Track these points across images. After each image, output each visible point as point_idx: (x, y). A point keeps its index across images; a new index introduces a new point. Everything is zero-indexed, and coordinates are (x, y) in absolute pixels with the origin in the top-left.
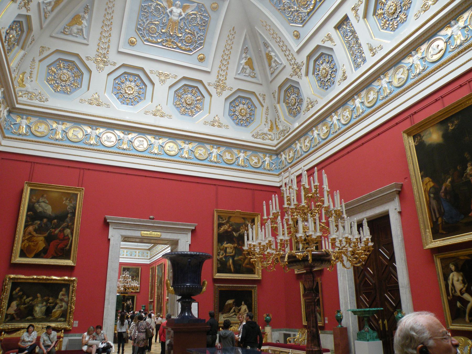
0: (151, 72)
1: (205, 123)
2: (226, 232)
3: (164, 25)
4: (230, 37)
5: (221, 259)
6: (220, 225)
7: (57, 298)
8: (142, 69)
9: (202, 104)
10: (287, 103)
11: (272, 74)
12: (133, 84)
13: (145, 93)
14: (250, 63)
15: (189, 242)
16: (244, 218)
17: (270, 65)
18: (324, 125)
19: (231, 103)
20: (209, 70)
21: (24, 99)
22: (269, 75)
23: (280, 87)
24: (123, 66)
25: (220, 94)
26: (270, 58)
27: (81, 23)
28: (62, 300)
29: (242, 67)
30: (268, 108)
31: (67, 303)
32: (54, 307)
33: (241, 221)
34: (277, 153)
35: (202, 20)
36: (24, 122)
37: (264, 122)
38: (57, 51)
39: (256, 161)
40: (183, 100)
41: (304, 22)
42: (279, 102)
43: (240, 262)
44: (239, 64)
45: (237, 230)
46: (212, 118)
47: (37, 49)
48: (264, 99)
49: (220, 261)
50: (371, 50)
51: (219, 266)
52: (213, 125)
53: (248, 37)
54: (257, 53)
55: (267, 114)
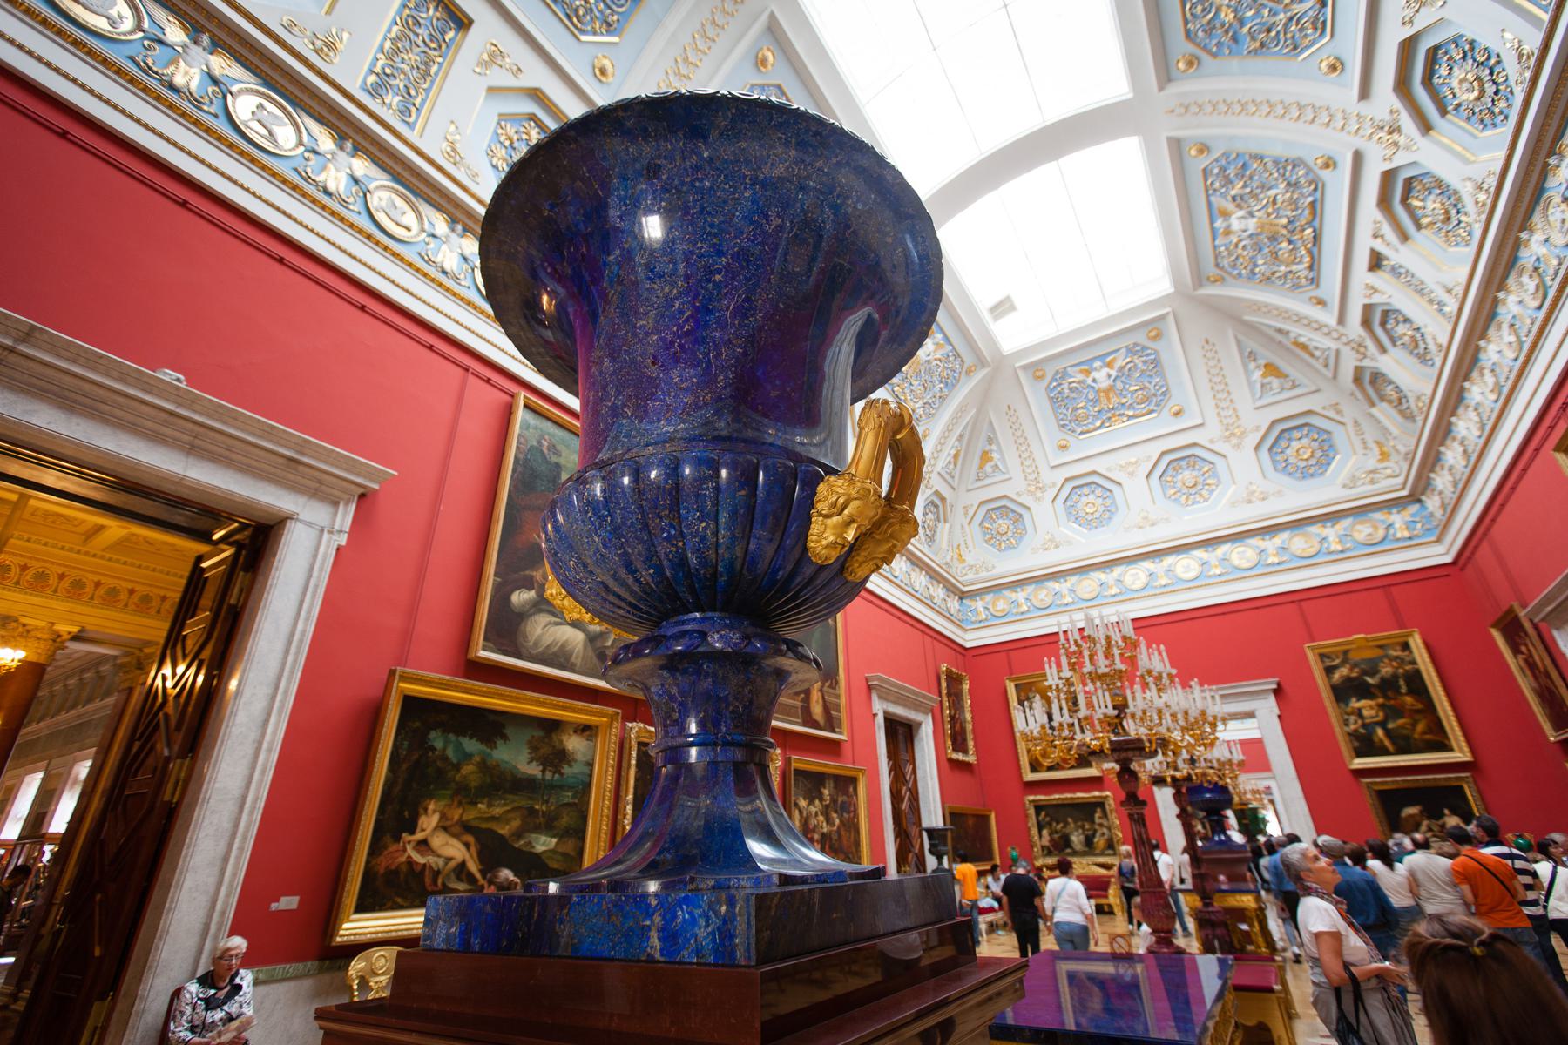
0: (1109, 469)
1: (1233, 504)
2: (1348, 679)
3: (1095, 401)
4: (1209, 355)
5: (1356, 730)
6: (1329, 671)
7: (1093, 822)
8: (1094, 472)
9: (1215, 475)
10: (1390, 402)
11: (1326, 366)
12: (1092, 497)
13: (1114, 503)
14: (1271, 369)
15: (1277, 711)
16: (1380, 647)
17: (1312, 355)
18: (1454, 439)
19: (1270, 450)
20: (1199, 421)
21: (970, 576)
22: (1324, 370)
23: (1357, 380)
24: (1067, 480)
25: (1238, 446)
26: (1304, 347)
27: (991, 459)
28: (1101, 825)
29: (1258, 386)
30: (1356, 423)
31: (1109, 829)
32: (1094, 835)
33: (1379, 652)
34: (1415, 497)
35: (1145, 362)
36: (979, 604)
37: (1360, 451)
38: (982, 503)
39: (1370, 530)
40: (1179, 485)
41: (1314, 281)
42: (1373, 404)
43: (1405, 732)
44: (1251, 384)
45: (1373, 672)
46: (1247, 488)
47: (960, 512)
48: (1339, 412)
49: (1354, 735)
50: (1449, 291)
51: (1356, 744)
52: (1250, 502)
53: (1241, 337)
54: (1275, 354)
55: (1360, 433)
